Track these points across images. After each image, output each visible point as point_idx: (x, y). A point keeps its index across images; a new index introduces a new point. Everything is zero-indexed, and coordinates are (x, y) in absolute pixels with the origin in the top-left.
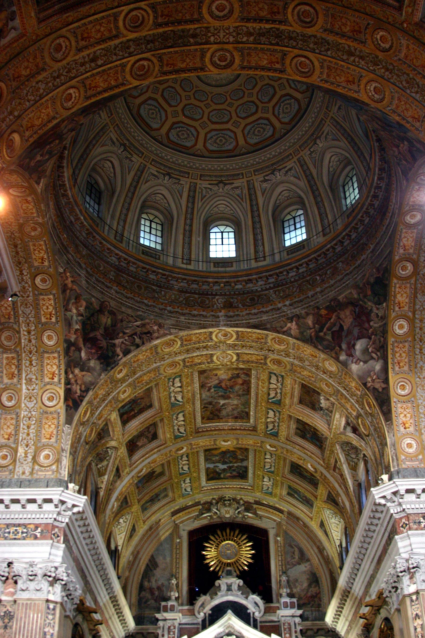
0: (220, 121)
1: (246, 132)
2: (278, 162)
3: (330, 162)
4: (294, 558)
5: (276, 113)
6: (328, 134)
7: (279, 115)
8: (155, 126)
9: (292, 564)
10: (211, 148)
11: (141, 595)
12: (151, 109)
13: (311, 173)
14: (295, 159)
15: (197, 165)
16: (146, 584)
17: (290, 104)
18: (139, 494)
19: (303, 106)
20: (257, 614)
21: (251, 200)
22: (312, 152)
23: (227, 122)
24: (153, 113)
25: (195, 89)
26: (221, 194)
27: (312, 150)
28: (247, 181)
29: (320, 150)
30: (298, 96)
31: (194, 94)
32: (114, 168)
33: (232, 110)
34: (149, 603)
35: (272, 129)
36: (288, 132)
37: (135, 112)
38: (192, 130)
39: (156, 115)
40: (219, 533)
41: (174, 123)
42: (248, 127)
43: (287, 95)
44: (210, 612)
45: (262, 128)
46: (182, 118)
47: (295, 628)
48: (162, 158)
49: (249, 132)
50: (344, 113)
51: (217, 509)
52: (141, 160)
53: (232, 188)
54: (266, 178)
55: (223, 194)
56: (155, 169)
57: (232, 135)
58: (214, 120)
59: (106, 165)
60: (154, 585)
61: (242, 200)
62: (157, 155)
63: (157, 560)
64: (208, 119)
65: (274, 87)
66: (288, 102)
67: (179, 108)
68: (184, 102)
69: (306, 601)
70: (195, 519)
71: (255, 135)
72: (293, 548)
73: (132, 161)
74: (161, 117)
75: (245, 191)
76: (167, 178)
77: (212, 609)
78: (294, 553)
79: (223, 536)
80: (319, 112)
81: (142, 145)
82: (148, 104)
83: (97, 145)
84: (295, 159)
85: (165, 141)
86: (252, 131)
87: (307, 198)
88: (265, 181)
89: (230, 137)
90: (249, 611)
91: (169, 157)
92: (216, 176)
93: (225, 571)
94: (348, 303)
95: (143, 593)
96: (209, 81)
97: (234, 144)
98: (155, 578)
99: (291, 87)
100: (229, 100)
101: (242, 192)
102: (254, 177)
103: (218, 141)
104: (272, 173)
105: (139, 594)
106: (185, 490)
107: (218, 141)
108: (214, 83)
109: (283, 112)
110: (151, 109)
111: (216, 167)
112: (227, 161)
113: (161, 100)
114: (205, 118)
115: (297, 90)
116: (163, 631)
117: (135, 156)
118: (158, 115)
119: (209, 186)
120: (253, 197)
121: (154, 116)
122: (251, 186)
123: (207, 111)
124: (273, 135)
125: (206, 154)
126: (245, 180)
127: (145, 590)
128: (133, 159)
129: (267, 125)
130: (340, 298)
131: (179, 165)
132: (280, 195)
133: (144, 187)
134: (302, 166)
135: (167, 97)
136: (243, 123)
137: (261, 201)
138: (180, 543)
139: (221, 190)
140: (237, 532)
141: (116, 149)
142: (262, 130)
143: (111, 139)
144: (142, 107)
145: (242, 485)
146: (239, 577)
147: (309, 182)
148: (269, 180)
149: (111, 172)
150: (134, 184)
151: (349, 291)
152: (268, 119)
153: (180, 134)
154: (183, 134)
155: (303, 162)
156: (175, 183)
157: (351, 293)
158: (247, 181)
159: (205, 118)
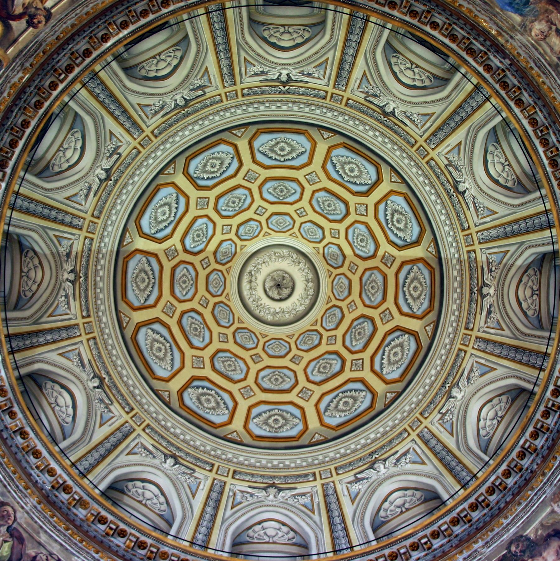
0: (276, 388)
1: (322, 406)
2: (382, 448)
3: (479, 420)
5: (377, 367)
6: (471, 370)
7: (382, 369)
8: (161, 373)
10: (258, 431)
12: (157, 341)
13: (445, 447)
14: (414, 435)
15: (230, 456)
17: (401, 345)
19: (425, 341)
21: (329, 511)
22: (444, 415)
23: (288, 391)
24: (160, 349)
25: (236, 325)
26: (270, 503)
27: (443, 411)
28: (323, 485)
29: (458, 404)
30: (414, 325)
31: (234, 334)
32: (74, 407)
33: (299, 369)
35: (369, 396)
36: (399, 395)
37: (129, 333)
38: (226, 396)
39: (165, 355)
41: (194, 378)
42: (327, 399)
43: (398, 328)
45: (351, 397)
46: (208, 372)
48: (167, 429)
49: (328, 405)
50: (498, 315)
52: (126, 417)
53: (294, 496)
54: (359, 476)
55: (274, 503)
56: (152, 442)
57: (297, 412)
58: (266, 384)
59: (61, 401)
61: (313, 511)
62: (157, 421)
64: (256, 382)
65: (372, 320)
66: (397, 341)
67: (207, 354)
68: (216, 345)
71: (339, 411)
73: (110, 411)
74: (172, 360)
75: (319, 499)
76: (170, 461)
80: (452, 344)
81: (134, 396)
82: (153, 330)
83: (53, 347)
84: (414, 435)
85: (175, 404)
86: (333, 405)
87: (440, 482)
88: (357, 480)
89: (292, 415)
91: (178, 431)
92: (262, 476)
94: (549, 536)
96: (262, 314)
97: (300, 427)
99: (401, 313)
100: (294, 351)
101: (312, 500)
102: (335, 478)
103: (270, 421)
104: (371, 467)
107: (270, 421)
108: (269, 318)
109: (390, 363)
110: (157, 341)
111: (264, 462)
112: (285, 455)
113: (176, 330)
114: (250, 380)
115: (412, 316)
117: (116, 404)
118: (169, 354)
119: (250, 490)
120: (334, 506)
121: (161, 354)
122: (331, 491)
123: (254, 368)
124: (371, 406)
125: (247, 439)
126: (319, 482)
128: (112, 407)
129: (361, 391)
130: (530, 532)
131: (196, 448)
132: (385, 500)
133: (124, 458)
134: (426, 443)
135: (187, 329)
136: (318, 391)
137: (348, 509)
139: (271, 497)
141: (84, 376)
142: (351, 401)
143: (79, 354)
144: (143, 331)
147: (441, 460)
148: (363, 479)
149: (68, 415)
150: (108, 445)
151: (549, 510)
152: (362, 381)
153: (203, 398)
154: (209, 401)
155: (428, 436)
156: (184, 473)
157: (553, 511)
158: (323, 485)
159: (250, 380)
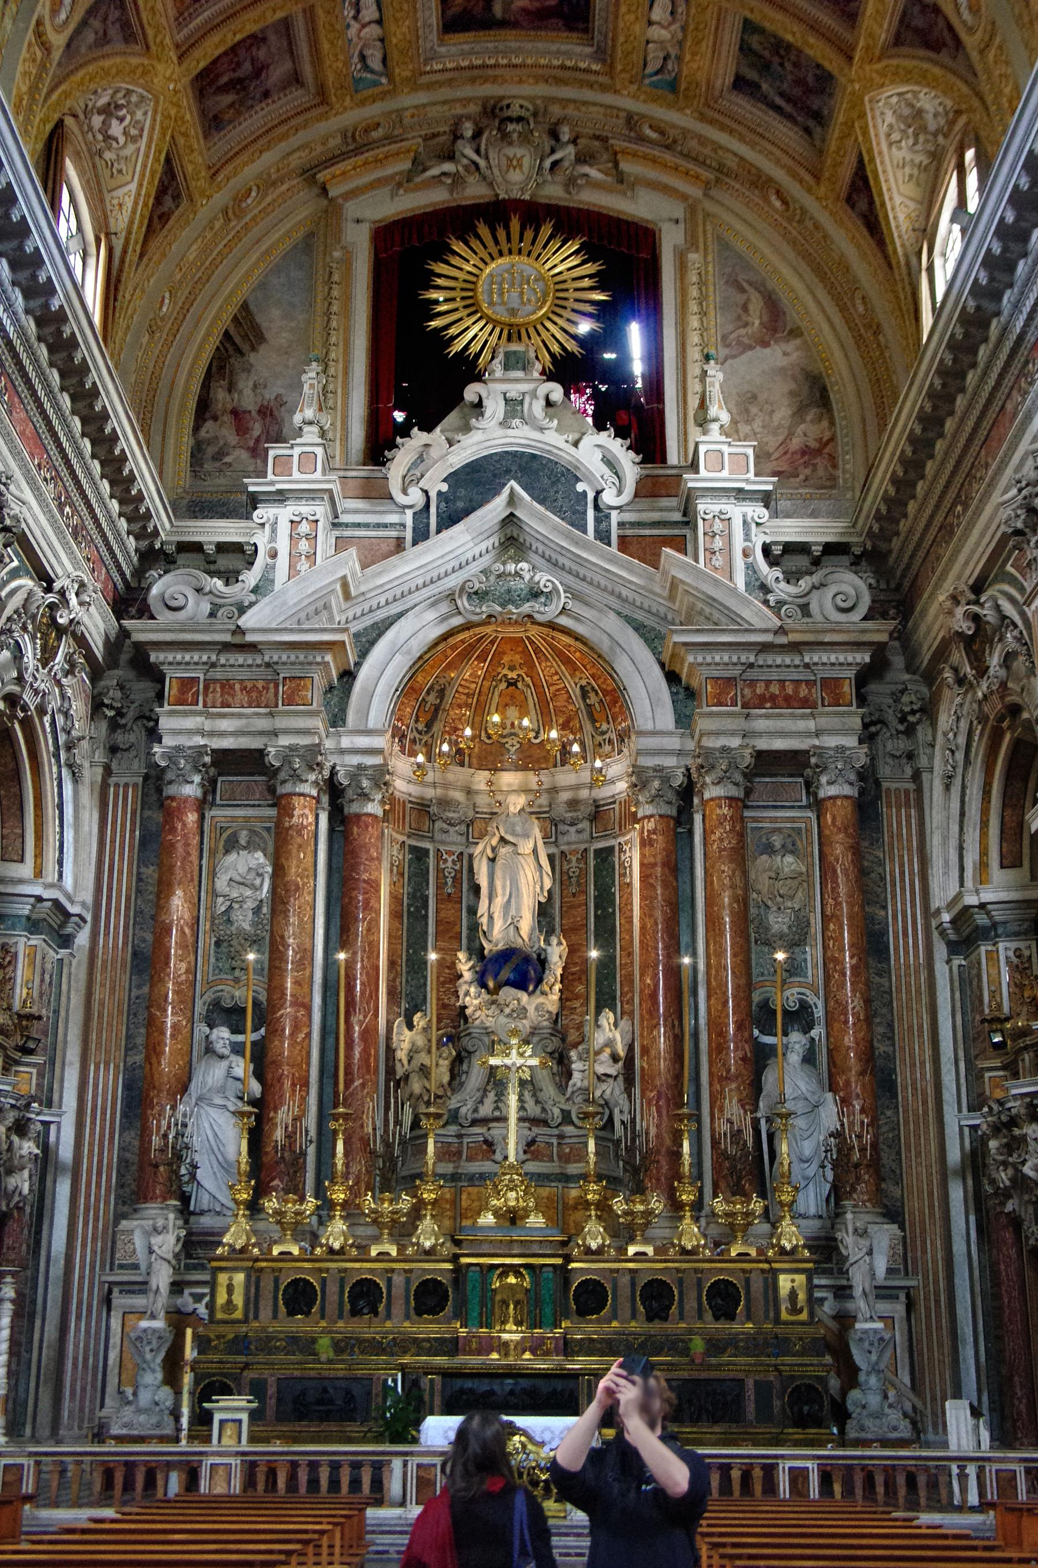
4: (746, 325)
9: (739, 343)
11: (203, 433)
16: (220, 396)
18: (182, 17)
20: (609, 498)
34: (227, 459)
40: (483, 230)
44: (444, 487)
47: (747, 537)
51: (478, 152)
60: (249, 401)
63: (260, 319)
69: (785, 467)
70: (399, 185)
72: (743, 290)
77: (452, 478)
78: (745, 308)
79: (497, 242)
90: (580, 487)
93: (501, 357)
95: (209, 428)
98: (253, 378)
105: (196, 429)
106: (363, 58)
116: (273, 539)
127: (215, 418)
138: (347, 262)
140: (546, 230)
145: (568, 54)
146: (550, 376)
